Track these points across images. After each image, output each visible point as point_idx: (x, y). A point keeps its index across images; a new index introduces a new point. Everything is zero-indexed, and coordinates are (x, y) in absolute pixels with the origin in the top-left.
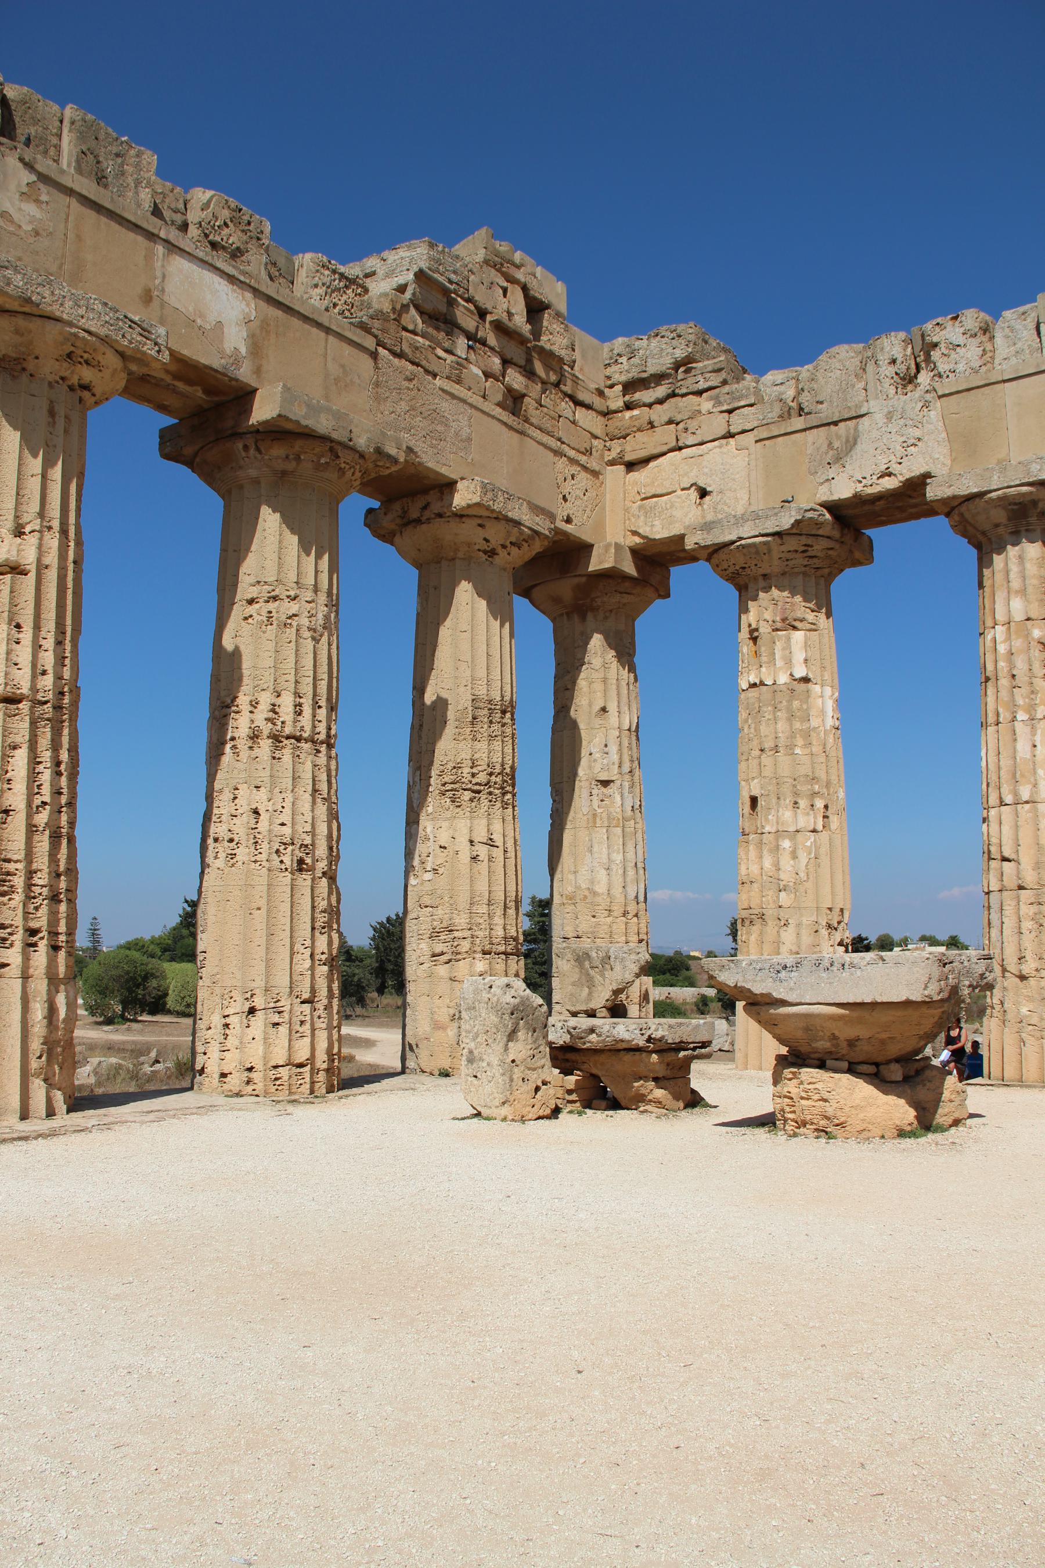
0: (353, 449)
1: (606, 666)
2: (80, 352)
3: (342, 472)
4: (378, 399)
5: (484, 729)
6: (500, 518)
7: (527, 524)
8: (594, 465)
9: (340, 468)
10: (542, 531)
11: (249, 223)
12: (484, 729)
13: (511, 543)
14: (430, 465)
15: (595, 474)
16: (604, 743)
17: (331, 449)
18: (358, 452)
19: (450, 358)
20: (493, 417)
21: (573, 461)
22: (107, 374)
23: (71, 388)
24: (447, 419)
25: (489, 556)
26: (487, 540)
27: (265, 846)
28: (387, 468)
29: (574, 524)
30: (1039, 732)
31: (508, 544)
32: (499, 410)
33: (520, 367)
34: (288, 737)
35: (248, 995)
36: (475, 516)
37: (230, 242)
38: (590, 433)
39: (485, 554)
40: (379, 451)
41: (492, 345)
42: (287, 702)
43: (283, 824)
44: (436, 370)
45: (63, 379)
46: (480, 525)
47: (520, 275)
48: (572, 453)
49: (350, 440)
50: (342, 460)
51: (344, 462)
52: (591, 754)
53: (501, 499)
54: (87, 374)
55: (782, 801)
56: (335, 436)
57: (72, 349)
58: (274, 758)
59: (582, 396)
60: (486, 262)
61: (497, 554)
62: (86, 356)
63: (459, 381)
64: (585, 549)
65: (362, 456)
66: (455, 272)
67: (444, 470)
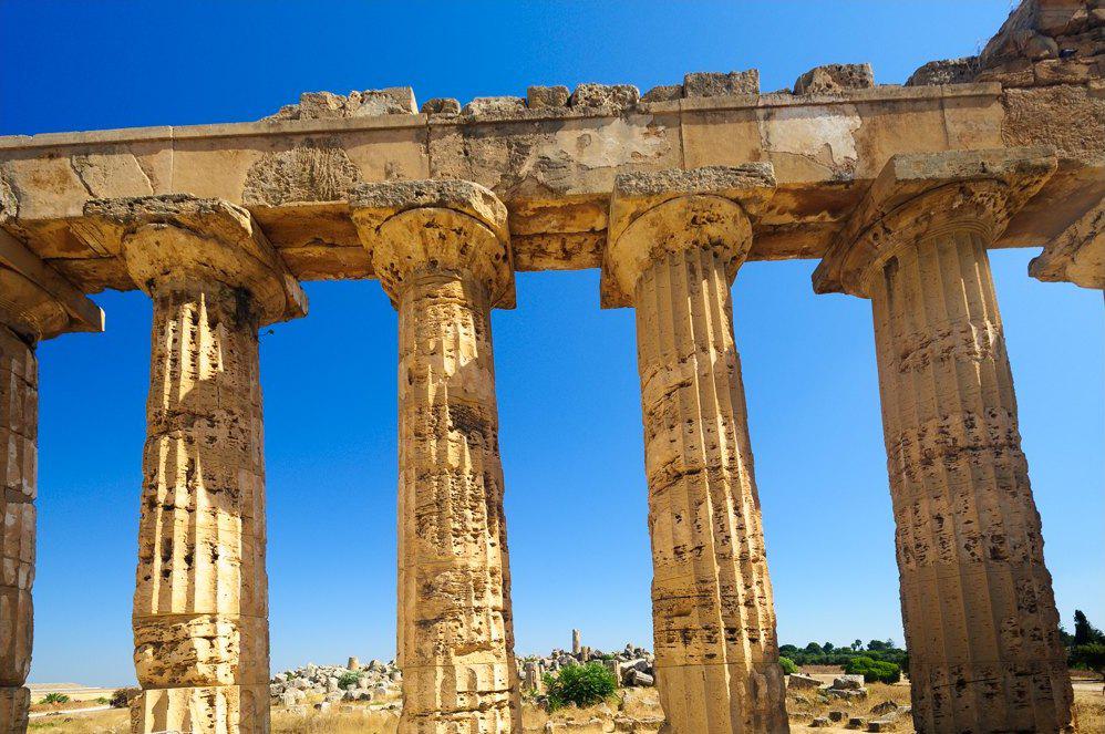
0: (991, 178)
2: (700, 214)
3: (980, 207)
9: (978, 204)
17: (962, 190)
22: (729, 222)
23: (705, 248)
27: (952, 545)
28: (1037, 182)
34: (962, 450)
35: (956, 670)
42: (956, 421)
43: (969, 522)
45: (696, 243)
50: (977, 194)
51: (981, 196)
54: (713, 230)
57: (694, 214)
58: (950, 470)
62: (705, 215)
65: (1001, 181)
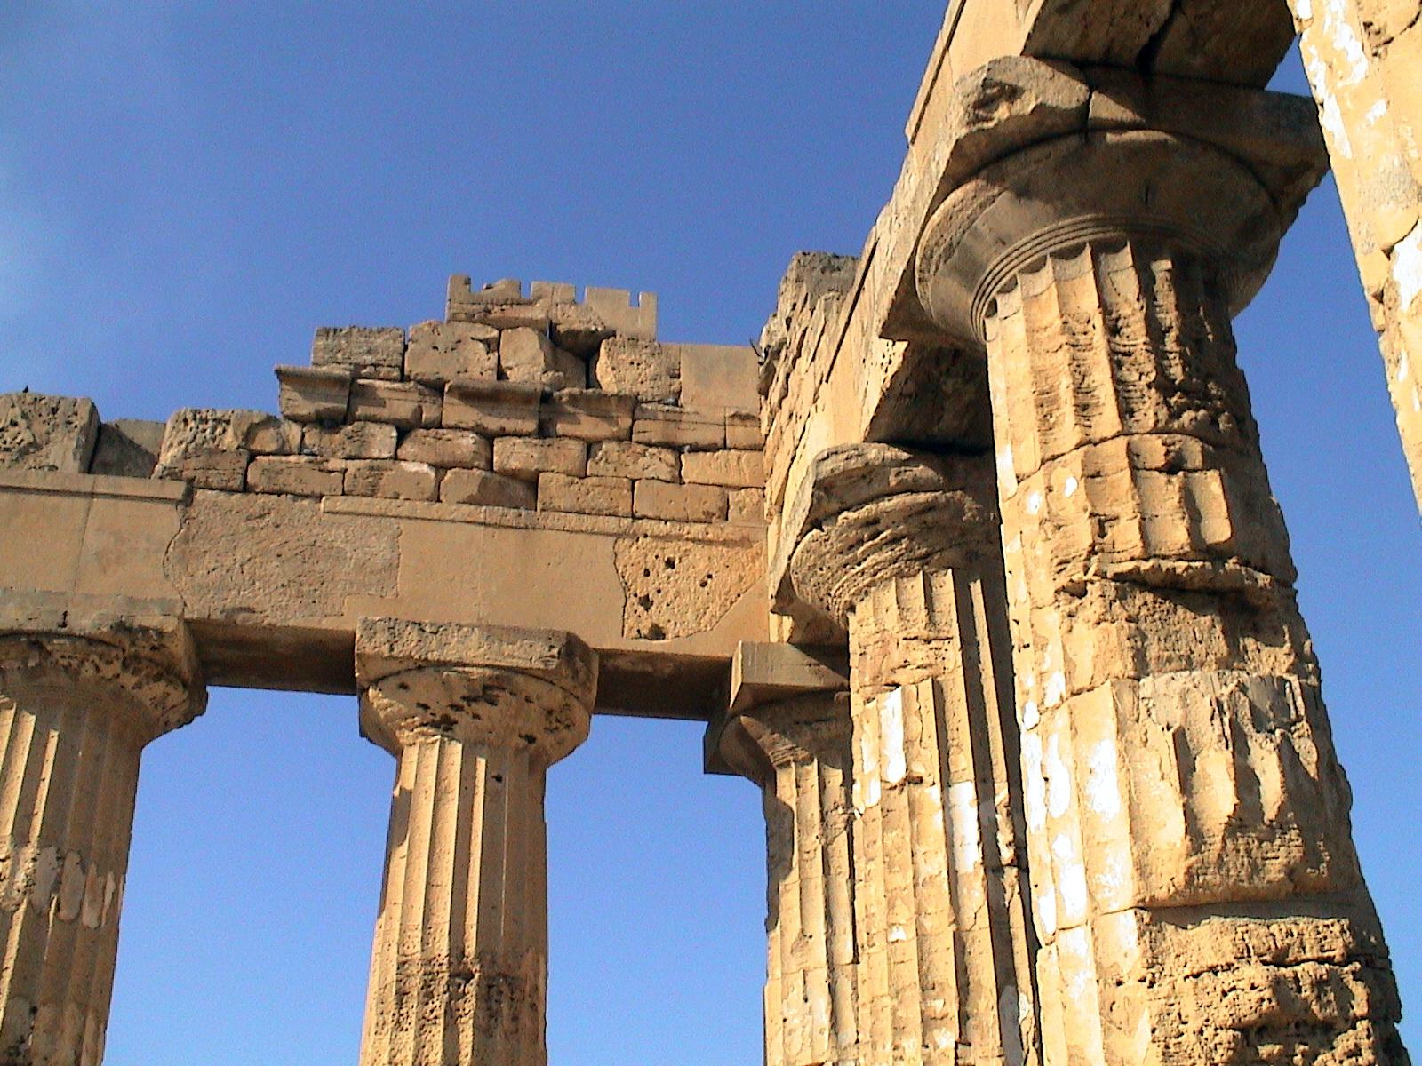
0: (69, 636)
1: (806, 856)
4: (184, 559)
5: (412, 1006)
6: (422, 666)
7: (475, 661)
8: (728, 530)
10: (523, 664)
11: (54, 411)
12: (412, 1006)
13: (464, 698)
14: (291, 623)
15: (745, 542)
16: (802, 996)
18: (81, 637)
19: (352, 466)
20: (453, 521)
21: (666, 538)
24: (339, 551)
25: (447, 730)
26: (426, 707)
29: (670, 636)
30: (1054, 740)
31: (458, 700)
32: (466, 508)
33: (529, 435)
36: (391, 675)
37: (18, 440)
38: (720, 486)
39: (439, 727)
40: (122, 627)
41: (452, 423)
44: (317, 491)
46: (404, 687)
47: (537, 313)
48: (663, 528)
49: (64, 625)
50: (57, 656)
51: (63, 657)
52: (785, 1020)
53: (415, 636)
55: (879, 1048)
56: (31, 627)
59: (687, 436)
60: (454, 318)
61: (456, 723)
63: (373, 492)
64: (722, 669)
65: (91, 640)
66: (369, 352)
67: (326, 624)
